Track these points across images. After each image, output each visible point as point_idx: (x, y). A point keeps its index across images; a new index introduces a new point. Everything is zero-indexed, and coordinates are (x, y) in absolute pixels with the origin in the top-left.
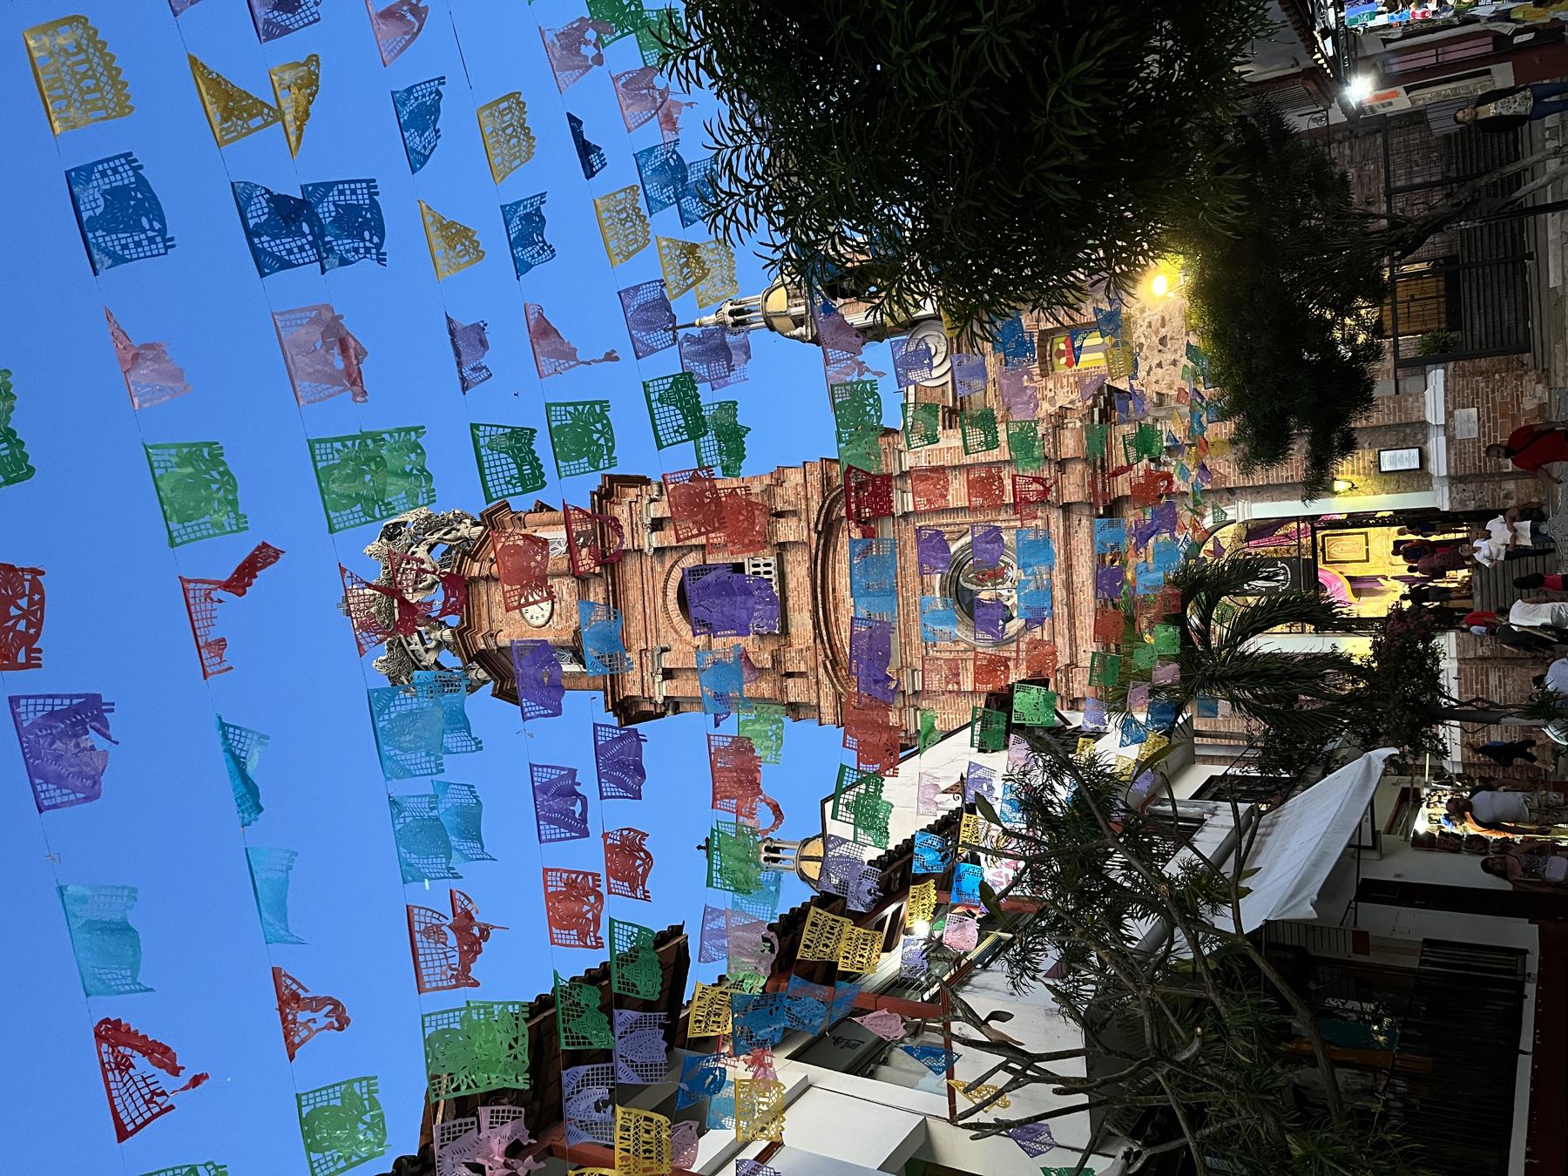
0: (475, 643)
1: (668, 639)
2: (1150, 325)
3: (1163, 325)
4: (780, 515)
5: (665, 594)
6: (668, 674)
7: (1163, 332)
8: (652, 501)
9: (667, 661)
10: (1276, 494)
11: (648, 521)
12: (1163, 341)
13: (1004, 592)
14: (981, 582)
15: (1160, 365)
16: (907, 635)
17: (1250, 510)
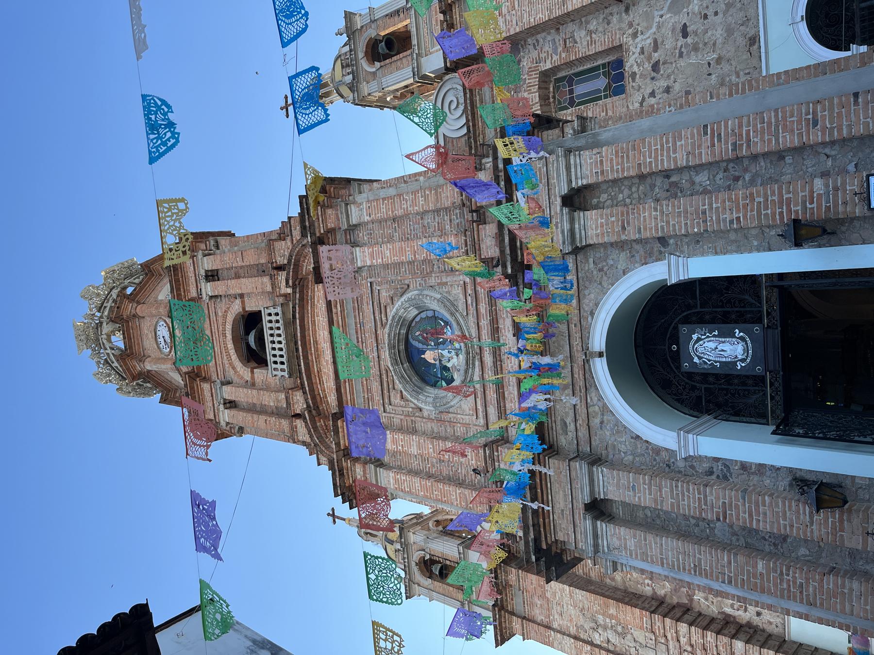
0: (135, 366)
1: (231, 374)
2: (642, 52)
3: (656, 48)
4: (280, 268)
5: (224, 335)
6: (231, 404)
7: (656, 56)
8: (205, 255)
9: (228, 393)
10: (720, 244)
11: (203, 273)
12: (655, 67)
13: (445, 353)
14: (425, 341)
15: (652, 94)
16: (369, 391)
17: (686, 267)
